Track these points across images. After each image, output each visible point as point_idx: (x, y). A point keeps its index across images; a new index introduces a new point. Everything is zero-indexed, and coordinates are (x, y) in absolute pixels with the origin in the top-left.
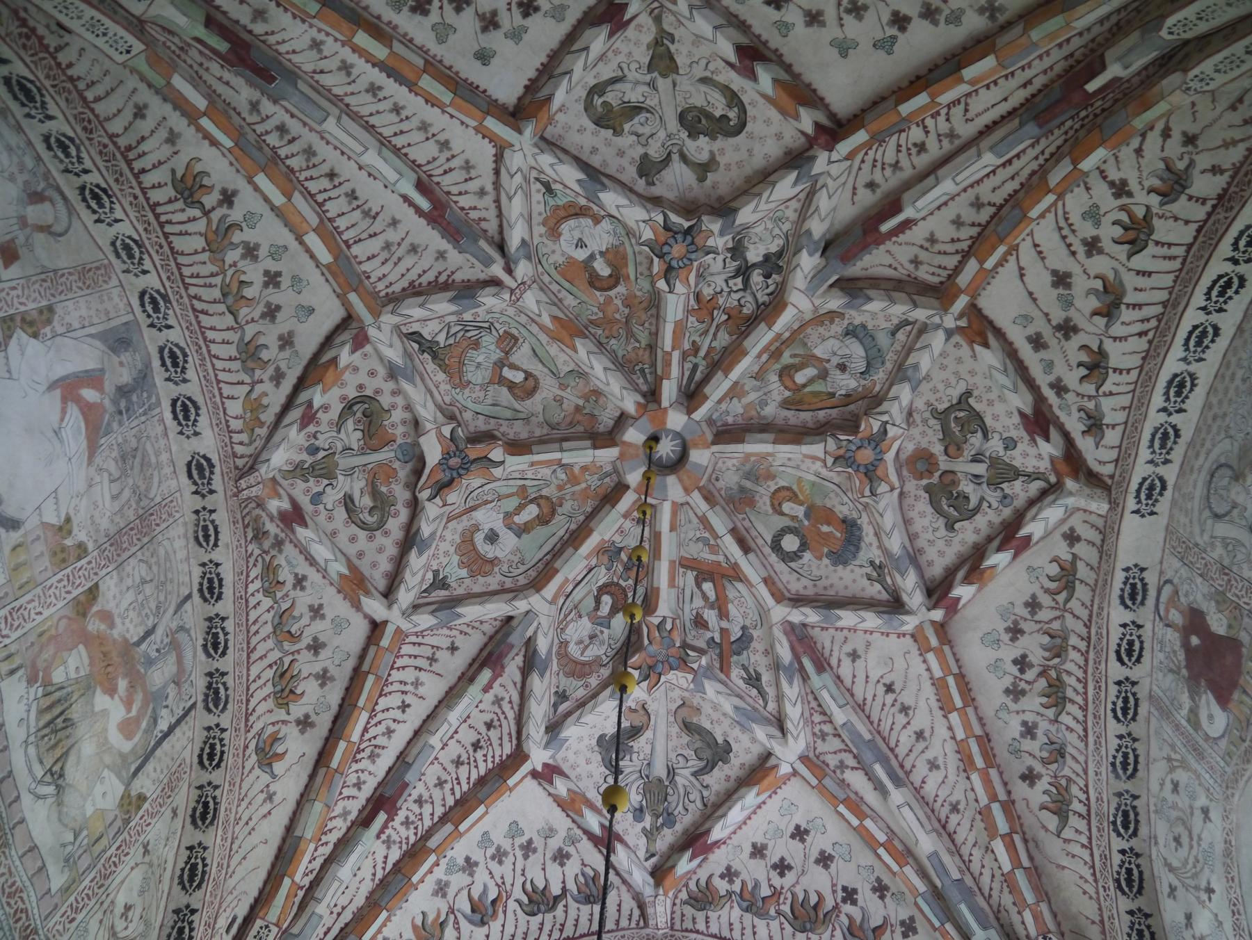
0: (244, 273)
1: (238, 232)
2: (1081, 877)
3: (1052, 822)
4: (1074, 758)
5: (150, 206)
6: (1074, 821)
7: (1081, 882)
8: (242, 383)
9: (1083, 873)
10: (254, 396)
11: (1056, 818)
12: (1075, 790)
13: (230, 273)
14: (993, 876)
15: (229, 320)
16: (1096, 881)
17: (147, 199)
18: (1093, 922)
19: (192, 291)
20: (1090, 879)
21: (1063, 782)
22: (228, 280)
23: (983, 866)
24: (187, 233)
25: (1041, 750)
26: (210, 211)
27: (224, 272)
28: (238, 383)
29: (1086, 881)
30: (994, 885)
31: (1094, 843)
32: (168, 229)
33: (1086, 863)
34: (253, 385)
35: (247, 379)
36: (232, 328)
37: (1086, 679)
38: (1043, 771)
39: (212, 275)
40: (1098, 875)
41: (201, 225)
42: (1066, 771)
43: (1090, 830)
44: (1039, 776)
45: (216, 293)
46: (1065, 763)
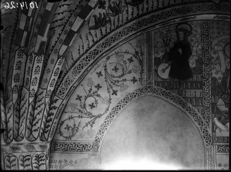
2: (83, 46)
3: (92, 24)
4: (119, 19)
6: (98, 31)
7: (81, 47)
9: (85, 45)
11: (94, 24)
12: (108, 25)
14: (62, 19)
16: (86, 52)
18: (73, 59)
20: (85, 49)
21: (108, 19)
23: (62, 13)
25: (113, 3)
29: (83, 48)
30: (59, 21)
31: (98, 44)
33: (89, 45)
37: (150, 13)
38: (107, 9)
40: (89, 52)
42: (112, 18)
43: (100, 40)
44: (104, 8)
46: (114, 16)
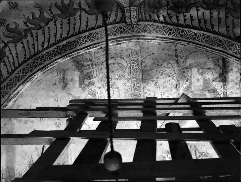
0: (28, 17)
1: (10, 26)
5: (10, 76)
8: (80, 16)
10: (87, 9)
13: (30, 26)
15: (51, 24)
17: (7, 78)
19: (40, 48)
22: (33, 26)
24: (17, 54)
26: (5, 43)
27: (30, 29)
28: (80, 19)
32: (17, 65)
34: (82, 9)
35: (78, 13)
36: (55, 22)
39: (32, 36)
41: (11, 46)
45: (40, 32)
